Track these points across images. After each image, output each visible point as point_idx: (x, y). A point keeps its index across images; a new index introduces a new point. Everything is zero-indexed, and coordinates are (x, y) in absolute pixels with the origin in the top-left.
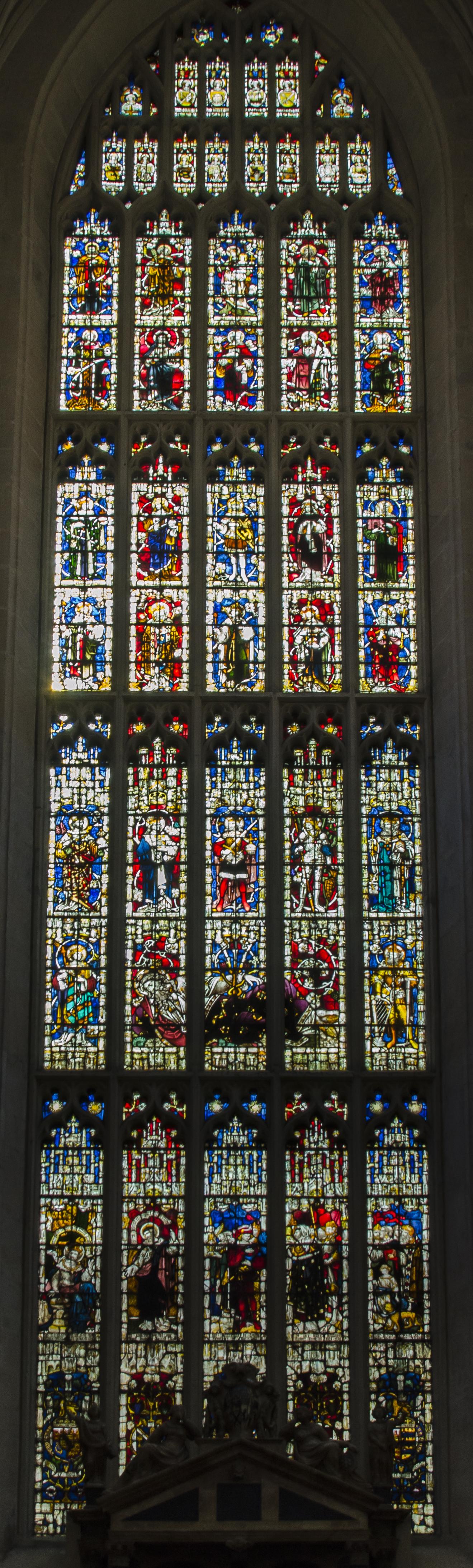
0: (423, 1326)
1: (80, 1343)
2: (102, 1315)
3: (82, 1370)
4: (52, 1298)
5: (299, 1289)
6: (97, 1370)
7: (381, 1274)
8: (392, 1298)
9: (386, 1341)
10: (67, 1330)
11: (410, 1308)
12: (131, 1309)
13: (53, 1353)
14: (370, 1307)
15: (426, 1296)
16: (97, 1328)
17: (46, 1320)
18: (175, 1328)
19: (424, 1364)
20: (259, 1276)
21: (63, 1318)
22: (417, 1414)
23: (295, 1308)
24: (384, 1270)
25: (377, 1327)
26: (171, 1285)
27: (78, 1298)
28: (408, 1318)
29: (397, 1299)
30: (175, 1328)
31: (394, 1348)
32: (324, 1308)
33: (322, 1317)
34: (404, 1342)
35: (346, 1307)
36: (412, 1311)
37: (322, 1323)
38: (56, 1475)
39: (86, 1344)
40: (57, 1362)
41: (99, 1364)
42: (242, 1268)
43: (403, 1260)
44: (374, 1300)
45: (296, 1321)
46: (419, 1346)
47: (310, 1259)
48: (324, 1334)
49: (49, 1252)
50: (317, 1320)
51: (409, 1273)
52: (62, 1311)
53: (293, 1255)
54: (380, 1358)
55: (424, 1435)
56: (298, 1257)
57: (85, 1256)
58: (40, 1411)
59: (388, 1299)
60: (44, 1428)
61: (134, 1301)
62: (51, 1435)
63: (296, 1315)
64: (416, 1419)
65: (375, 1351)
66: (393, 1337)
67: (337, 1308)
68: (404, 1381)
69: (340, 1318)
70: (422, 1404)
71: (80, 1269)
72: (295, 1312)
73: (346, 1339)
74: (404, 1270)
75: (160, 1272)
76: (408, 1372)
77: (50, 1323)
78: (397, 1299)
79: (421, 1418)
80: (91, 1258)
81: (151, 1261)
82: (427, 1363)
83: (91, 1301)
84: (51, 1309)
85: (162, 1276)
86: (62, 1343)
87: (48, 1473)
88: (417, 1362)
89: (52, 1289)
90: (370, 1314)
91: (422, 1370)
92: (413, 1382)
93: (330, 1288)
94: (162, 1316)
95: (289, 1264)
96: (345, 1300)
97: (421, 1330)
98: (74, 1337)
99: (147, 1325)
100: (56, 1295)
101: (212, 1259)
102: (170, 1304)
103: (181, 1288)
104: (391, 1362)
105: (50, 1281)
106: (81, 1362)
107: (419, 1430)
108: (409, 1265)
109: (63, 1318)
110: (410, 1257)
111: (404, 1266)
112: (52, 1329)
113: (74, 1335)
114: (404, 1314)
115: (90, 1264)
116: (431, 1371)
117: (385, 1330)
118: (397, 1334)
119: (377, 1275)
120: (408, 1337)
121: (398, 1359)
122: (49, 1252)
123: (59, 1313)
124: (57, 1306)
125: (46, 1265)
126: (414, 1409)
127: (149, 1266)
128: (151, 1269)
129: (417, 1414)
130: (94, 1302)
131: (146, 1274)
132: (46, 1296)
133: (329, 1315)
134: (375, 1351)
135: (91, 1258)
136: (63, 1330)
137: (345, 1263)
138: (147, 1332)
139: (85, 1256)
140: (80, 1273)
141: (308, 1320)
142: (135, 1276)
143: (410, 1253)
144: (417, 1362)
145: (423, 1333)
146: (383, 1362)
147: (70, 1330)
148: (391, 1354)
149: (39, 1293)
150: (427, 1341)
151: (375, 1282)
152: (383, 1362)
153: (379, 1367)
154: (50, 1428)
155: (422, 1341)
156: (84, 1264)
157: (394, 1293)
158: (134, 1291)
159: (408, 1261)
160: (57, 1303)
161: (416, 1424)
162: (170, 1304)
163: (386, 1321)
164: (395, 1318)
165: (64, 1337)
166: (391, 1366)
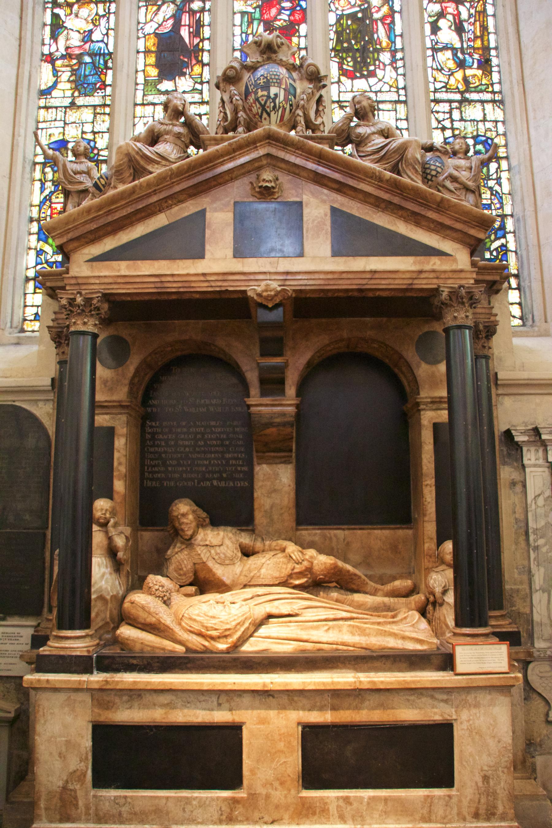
0: (492, 85)
1: (87, 106)
2: (114, 76)
3: (90, 136)
4: (57, 59)
5: (345, 45)
6: (106, 136)
7: (439, 29)
8: (455, 55)
9: (450, 102)
10: (73, 94)
11: (475, 65)
12: (149, 69)
13: (55, 120)
14: (429, 60)
15: (493, 53)
16: (109, 90)
17: (50, 84)
18: (198, 87)
19: (496, 126)
20: (298, 31)
21: (69, 81)
22: (491, 183)
23: (340, 65)
24: (442, 23)
25: (438, 85)
26: (196, 41)
27: (87, 59)
28: (474, 76)
29: (459, 55)
30: (198, 87)
31: (459, 108)
32: (375, 65)
33: (373, 74)
34: (470, 102)
35: (400, 64)
36: (478, 68)
37: (372, 81)
38: (53, 260)
39: (95, 107)
40: (61, 130)
41: (109, 130)
42: (278, 23)
43: (464, 15)
44: (433, 55)
45: (343, 79)
46: (489, 107)
47: (357, 12)
48: (376, 92)
49: (56, 11)
50: (366, 77)
51: (472, 28)
52: (69, 74)
53: (337, 9)
54: (444, 120)
55: (502, 207)
56: (343, 10)
57: (97, 14)
58: (38, 185)
59: (449, 54)
60: (42, 203)
61: (152, 60)
62: (49, 213)
63: (344, 73)
64: (491, 189)
65: (437, 112)
66: (458, 97)
67: (391, 64)
68: (474, 146)
69: (394, 75)
70: (497, 172)
71: (91, 27)
72: (340, 68)
73: (403, 98)
74: (465, 25)
75: (182, 29)
76: (478, 136)
77: (54, 86)
78: (459, 55)
79: (497, 188)
80: (104, 16)
81: (173, 16)
82: (500, 125)
83: (102, 62)
84: (55, 72)
85: (184, 33)
86: (66, 107)
87: (43, 257)
88: (489, 125)
89: (57, 50)
90: (430, 70)
91: (494, 134)
92: (484, 147)
93: (380, 44)
94: (184, 74)
95: (332, 19)
96: (399, 55)
97: (490, 89)
98: (80, 101)
99: (167, 85)
100: (63, 57)
101: (243, 13)
102: (194, 62)
103: (206, 45)
104: (456, 125)
105: (56, 41)
106: (88, 128)
107: (496, 201)
108: (472, 20)
109: (69, 81)
110: (472, 11)
111: (465, 21)
112: (55, 93)
113: (81, 98)
114: (469, 72)
115: (103, 21)
116: (505, 135)
117: (447, 88)
118: (462, 93)
119: (435, 29)
120: (474, 96)
121: (465, 121)
122: (56, 11)
123: (65, 76)
124: (63, 69)
125: (52, 25)
126: (488, 178)
127: (171, 22)
128: (174, 25)
129: (491, 183)
130: (106, 62)
131: (166, 31)
132: (50, 59)
133: (380, 73)
134: (437, 112)
135: (104, 16)
136: (69, 93)
137: (397, 16)
138: (167, 92)
139: (97, 14)
140: (91, 32)
141: (357, 78)
142: (154, 33)
143: (471, 6)
144: (489, 125)
145: (493, 92)
146: (447, 124)
147: (76, 94)
148: (456, 115)
149: (43, 55)
150: (498, 101)
151: (433, 37)
152: (447, 124)
153: (443, 129)
154: (48, 203)
155: (493, 101)
156: (95, 23)
157: (456, 49)
158: (153, 49)
159: (470, 16)
160: (63, 66)
161: (492, 194)
162: (194, 62)
163: (449, 79)
164: (459, 75)
165: (70, 100)
166: (457, 129)
